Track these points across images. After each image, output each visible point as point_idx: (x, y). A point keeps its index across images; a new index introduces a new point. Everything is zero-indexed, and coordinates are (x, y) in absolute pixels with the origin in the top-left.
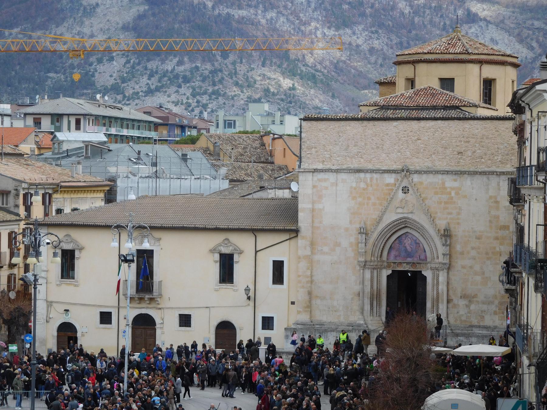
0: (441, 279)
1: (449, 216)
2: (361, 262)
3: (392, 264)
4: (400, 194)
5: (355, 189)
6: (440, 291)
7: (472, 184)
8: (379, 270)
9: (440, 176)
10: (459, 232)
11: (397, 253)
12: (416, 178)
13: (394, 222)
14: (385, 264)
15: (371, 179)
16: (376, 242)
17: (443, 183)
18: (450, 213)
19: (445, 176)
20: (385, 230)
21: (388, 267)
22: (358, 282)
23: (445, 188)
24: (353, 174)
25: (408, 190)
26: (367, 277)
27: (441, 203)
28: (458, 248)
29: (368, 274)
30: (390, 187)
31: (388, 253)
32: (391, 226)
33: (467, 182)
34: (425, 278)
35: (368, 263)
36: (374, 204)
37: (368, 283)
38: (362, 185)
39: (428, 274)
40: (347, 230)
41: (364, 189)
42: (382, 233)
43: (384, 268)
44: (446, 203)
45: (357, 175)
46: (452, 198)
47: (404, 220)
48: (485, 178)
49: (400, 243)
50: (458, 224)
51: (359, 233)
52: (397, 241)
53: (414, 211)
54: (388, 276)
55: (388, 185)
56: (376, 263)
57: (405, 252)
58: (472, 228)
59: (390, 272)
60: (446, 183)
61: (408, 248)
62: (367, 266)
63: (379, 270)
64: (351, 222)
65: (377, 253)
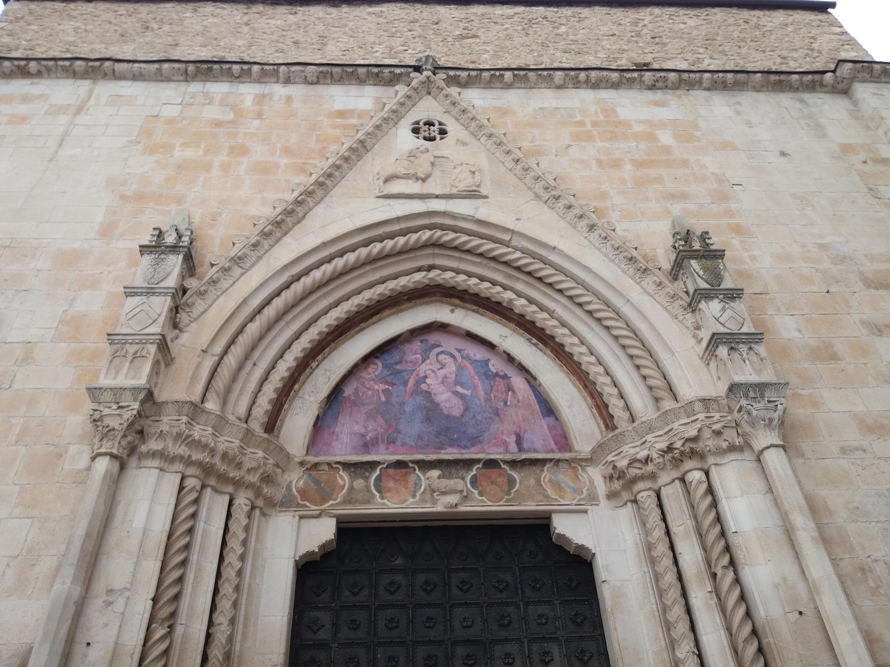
0: (744, 508)
1: (676, 209)
2: (118, 392)
3: (343, 478)
4: (403, 139)
5: (171, 121)
6: (769, 606)
7: (738, 113)
8: (242, 500)
9: (588, 95)
10: (753, 258)
11: (375, 427)
12: (476, 98)
14: (295, 478)
15: (261, 99)
16: (253, 329)
17: (609, 111)
18: (684, 197)
19: (606, 95)
20: (317, 275)
21: (318, 493)
22: (47, 563)
23: (627, 124)
24: (173, 85)
25: (443, 132)
26: (138, 520)
27: (616, 164)
28: (787, 327)
29: (150, 500)
30: (354, 121)
31: (319, 425)
32: (351, 257)
33: (716, 110)
35: (167, 422)
36: (264, 169)
37: (131, 571)
38: (213, 112)
39: (606, 534)
40: (69, 259)
41: (218, 124)
42: (297, 288)
43: (287, 503)
44: (638, 164)
45: (195, 87)
46: (667, 150)
47: (426, 235)
48: (786, 100)
49: (395, 376)
50: (738, 230)
51: (144, 249)
52: (377, 368)
53: (484, 192)
54: (309, 571)
55: (342, 114)
56: (229, 442)
57: (428, 419)
58: (823, 247)
60: (619, 110)
61: (444, 397)
62: (154, 445)
63: (242, 500)
64: (107, 231)
65: (250, 397)
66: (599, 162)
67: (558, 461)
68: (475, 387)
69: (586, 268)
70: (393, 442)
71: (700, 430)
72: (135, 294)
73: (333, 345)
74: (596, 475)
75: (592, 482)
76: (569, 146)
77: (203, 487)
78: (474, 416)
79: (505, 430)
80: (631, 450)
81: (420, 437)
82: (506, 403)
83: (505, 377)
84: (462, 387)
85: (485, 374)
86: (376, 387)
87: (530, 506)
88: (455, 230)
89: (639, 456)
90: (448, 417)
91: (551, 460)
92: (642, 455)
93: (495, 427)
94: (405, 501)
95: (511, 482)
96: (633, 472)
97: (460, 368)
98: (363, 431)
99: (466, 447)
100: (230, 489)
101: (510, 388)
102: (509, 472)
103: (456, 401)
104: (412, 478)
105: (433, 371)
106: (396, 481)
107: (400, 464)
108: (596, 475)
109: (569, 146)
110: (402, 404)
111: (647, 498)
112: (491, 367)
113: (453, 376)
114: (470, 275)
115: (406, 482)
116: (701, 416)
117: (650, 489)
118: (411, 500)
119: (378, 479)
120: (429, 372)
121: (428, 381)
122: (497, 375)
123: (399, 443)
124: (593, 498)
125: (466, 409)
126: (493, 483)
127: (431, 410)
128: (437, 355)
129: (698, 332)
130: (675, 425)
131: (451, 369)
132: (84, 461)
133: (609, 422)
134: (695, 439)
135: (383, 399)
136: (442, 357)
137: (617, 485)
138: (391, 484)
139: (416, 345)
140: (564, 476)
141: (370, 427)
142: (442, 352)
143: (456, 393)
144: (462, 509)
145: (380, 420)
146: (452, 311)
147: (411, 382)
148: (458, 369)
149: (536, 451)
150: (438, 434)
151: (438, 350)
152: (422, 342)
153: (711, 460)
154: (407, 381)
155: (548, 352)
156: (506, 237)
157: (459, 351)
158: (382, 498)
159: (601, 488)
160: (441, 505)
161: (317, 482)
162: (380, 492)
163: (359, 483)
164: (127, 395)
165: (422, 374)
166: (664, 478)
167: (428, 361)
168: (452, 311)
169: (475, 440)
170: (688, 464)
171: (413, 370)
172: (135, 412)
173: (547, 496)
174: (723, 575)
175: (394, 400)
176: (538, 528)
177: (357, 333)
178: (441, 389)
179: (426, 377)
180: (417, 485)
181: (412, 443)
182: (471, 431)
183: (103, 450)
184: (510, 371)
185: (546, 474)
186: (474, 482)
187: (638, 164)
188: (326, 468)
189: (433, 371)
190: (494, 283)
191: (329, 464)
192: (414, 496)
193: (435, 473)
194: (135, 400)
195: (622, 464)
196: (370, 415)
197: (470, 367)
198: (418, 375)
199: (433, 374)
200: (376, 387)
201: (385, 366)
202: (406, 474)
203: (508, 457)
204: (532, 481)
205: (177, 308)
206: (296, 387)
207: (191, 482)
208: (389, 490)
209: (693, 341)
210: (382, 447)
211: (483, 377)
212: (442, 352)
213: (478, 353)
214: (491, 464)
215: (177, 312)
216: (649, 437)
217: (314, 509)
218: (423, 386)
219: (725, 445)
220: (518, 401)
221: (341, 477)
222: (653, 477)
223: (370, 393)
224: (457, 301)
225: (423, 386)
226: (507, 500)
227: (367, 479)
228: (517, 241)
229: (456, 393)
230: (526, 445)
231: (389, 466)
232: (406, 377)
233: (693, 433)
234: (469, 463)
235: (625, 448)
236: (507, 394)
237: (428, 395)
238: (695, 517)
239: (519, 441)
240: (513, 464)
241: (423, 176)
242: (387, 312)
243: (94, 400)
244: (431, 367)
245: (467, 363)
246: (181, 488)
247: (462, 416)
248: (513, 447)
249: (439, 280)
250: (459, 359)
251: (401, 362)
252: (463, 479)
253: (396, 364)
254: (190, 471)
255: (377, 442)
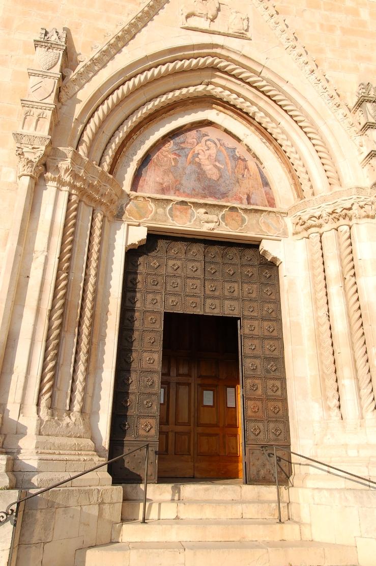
2: (31, 138)
3: (152, 206)
11: (168, 180)
13: (174, 53)
27: (331, 29)
34: (271, 266)
39: (289, 253)
44: (345, 31)
49: (180, 151)
51: (37, 44)
53: (249, 35)
59: (139, 235)
61: (208, 167)
66: (322, 26)
67: (270, 212)
68: (227, 164)
69: (304, 98)
70: (178, 190)
71: (353, 205)
72: (35, 75)
73: (146, 126)
74: (289, 221)
75: (286, 226)
76: (304, 10)
77: (80, 201)
78: (225, 181)
79: (242, 190)
80: (310, 211)
81: (194, 190)
82: (243, 176)
83: (244, 160)
84: (219, 162)
85: (233, 156)
86: (169, 156)
87: (251, 234)
88: (227, 59)
89: (315, 215)
90: (210, 179)
91: (266, 211)
92: (317, 215)
93: (236, 189)
94: (185, 223)
95: (243, 220)
96: (310, 222)
97: (219, 151)
98: (161, 181)
99: (218, 198)
100: (93, 205)
101: (246, 167)
102: (242, 215)
103: (215, 170)
104: (190, 211)
105: (203, 151)
106: (181, 212)
107: (183, 203)
108: (289, 221)
109: (304, 10)
110: (184, 169)
111: (315, 238)
112: (237, 153)
113: (214, 155)
114: (232, 91)
115: (186, 213)
116: (355, 197)
117: (318, 232)
118: (188, 223)
119: (171, 210)
120: (200, 151)
121: (200, 156)
122: (240, 158)
123: (181, 191)
124: (285, 234)
125: (221, 177)
126: (233, 219)
127: (201, 175)
128: (206, 141)
129: (361, 148)
130: (339, 200)
131: (213, 151)
132: (12, 178)
133: (300, 194)
134: (350, 209)
135: (173, 164)
136: (208, 143)
137: (299, 228)
138: (178, 213)
139: (194, 133)
140: (271, 220)
141: (165, 180)
142: (209, 140)
143: (215, 166)
144: (215, 231)
145: (171, 175)
146: (218, 114)
147: (190, 156)
148: (217, 152)
149: (257, 205)
150: (204, 189)
151: (206, 138)
152: (197, 131)
153: (354, 221)
154: (188, 155)
155: (271, 148)
156: (259, 69)
157: (219, 140)
158: (173, 220)
159: (291, 228)
160: (205, 228)
161: (137, 207)
162: (172, 217)
163: (160, 211)
164: (37, 140)
165: (196, 152)
166: (326, 227)
167: (200, 144)
168: (218, 114)
169: (224, 195)
170: (342, 221)
171: (191, 149)
172: (43, 152)
173: (261, 230)
174: (350, 280)
175: (179, 165)
176: (254, 245)
177: (160, 120)
178: (207, 162)
179: (199, 154)
180: (192, 215)
181: (189, 192)
182: (222, 189)
183: (25, 173)
184: (248, 157)
185: (263, 218)
186: (223, 218)
187: (345, 31)
188: (142, 199)
189: (203, 151)
190: (246, 99)
191: (144, 198)
192: (190, 221)
193: (202, 210)
194: (42, 144)
195: (305, 217)
196: (166, 172)
197: (225, 152)
198: (194, 152)
199: (202, 153)
200: (169, 156)
201: (175, 144)
202: (186, 209)
203: (244, 207)
204: (254, 222)
205: (60, 88)
206: (125, 149)
207: (74, 198)
208: (177, 217)
209: (357, 153)
210: (172, 192)
211: (232, 158)
212: (209, 140)
213: (230, 142)
214: (233, 209)
215: (60, 92)
216: (323, 205)
217: (136, 222)
218: (197, 159)
219: (364, 214)
220: (250, 176)
221: (150, 205)
222: (320, 226)
223: (165, 159)
224: (221, 109)
225: (197, 159)
226: (240, 230)
227: (164, 208)
228: (265, 74)
229: (215, 166)
230: (252, 201)
231: (177, 203)
232: (187, 152)
233: (349, 206)
234: (222, 207)
235: (308, 210)
236: (244, 171)
237: (199, 165)
238: (340, 249)
239: (248, 199)
240: (245, 210)
241: (211, 17)
242: (178, 109)
243: (18, 141)
244: (202, 148)
245: (223, 149)
246: (69, 200)
247: (218, 180)
248: (245, 201)
249: (214, 93)
250: (219, 146)
251: (184, 142)
252: (217, 215)
253: (181, 143)
254: (73, 192)
255: (169, 189)
